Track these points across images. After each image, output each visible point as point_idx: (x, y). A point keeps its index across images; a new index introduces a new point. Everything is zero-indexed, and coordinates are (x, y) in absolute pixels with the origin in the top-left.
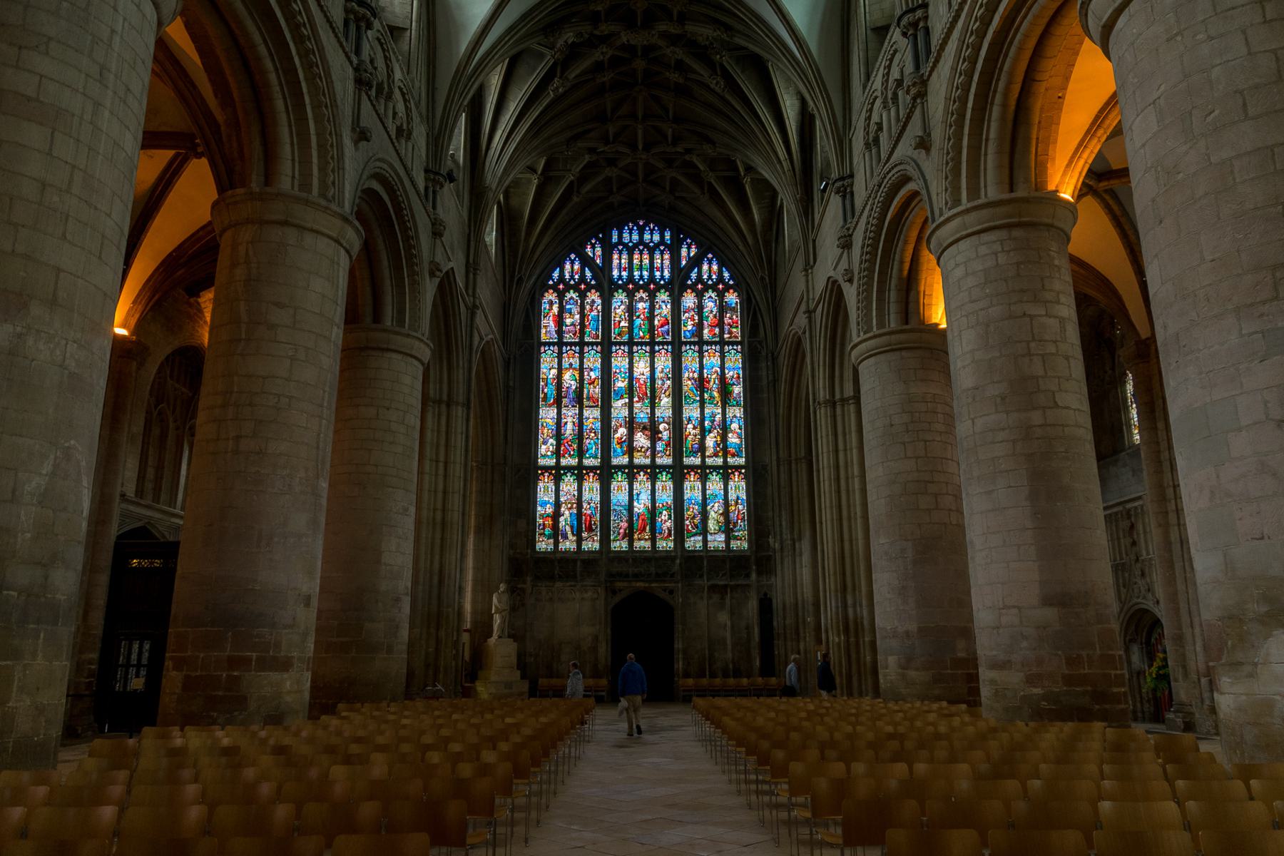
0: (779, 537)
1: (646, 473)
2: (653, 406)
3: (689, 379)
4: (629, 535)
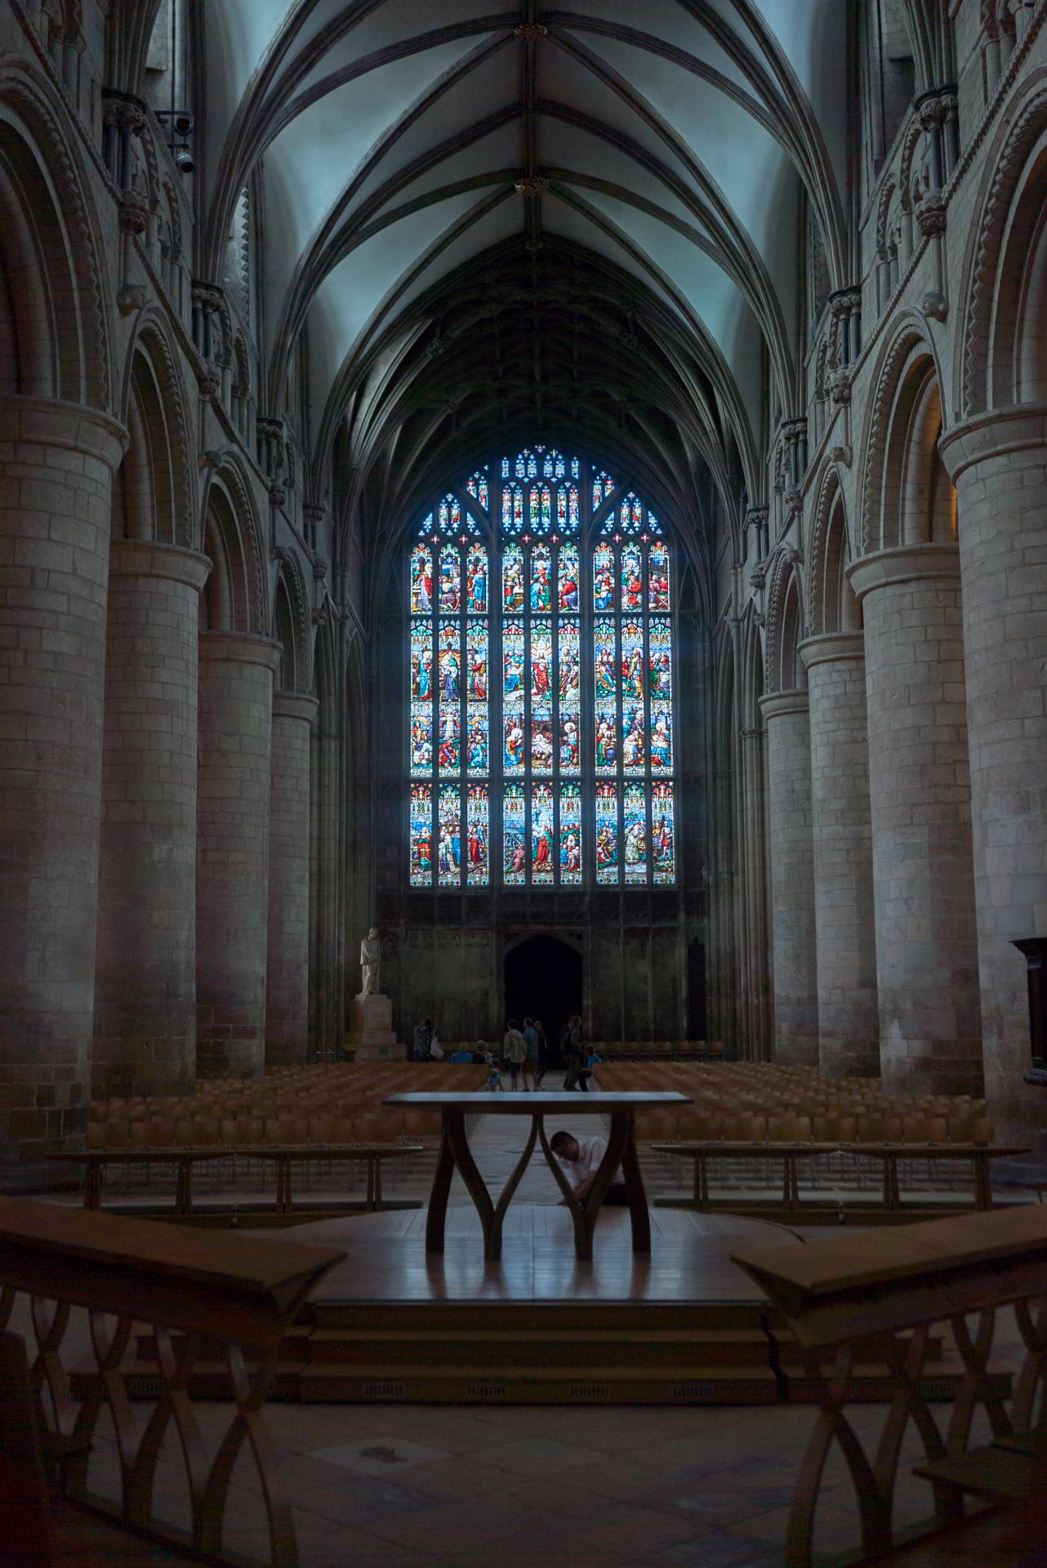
0: (713, 870)
1: (547, 787)
2: (556, 699)
3: (603, 663)
4: (527, 865)
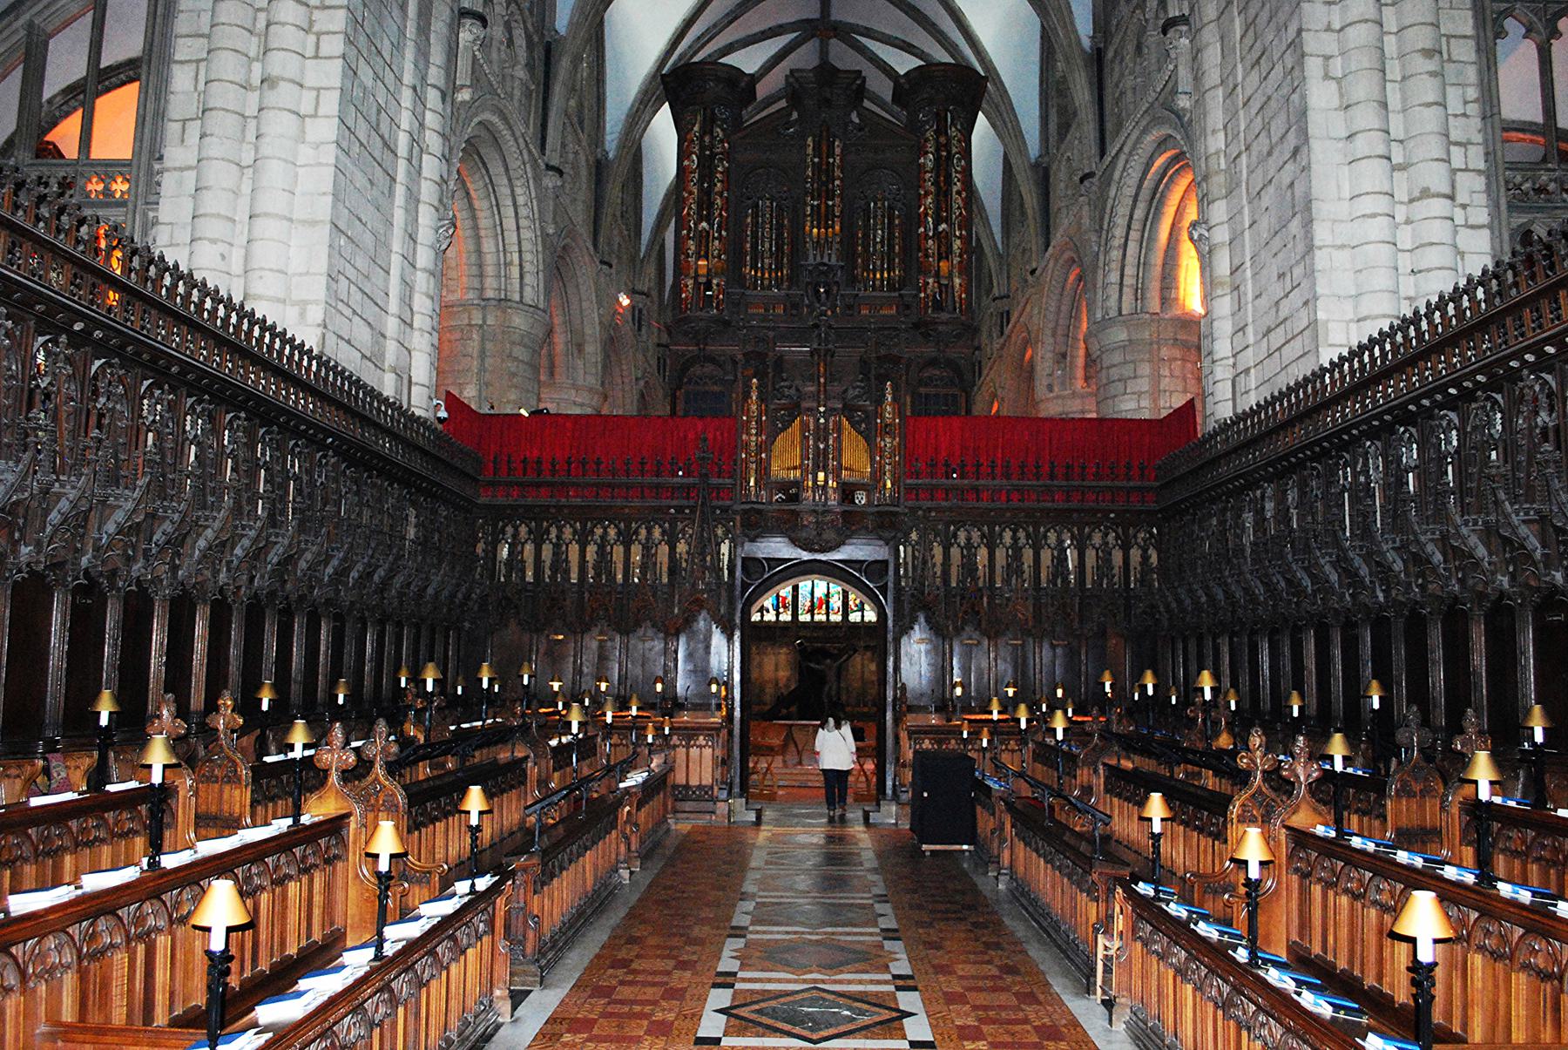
4: (811, 611)
